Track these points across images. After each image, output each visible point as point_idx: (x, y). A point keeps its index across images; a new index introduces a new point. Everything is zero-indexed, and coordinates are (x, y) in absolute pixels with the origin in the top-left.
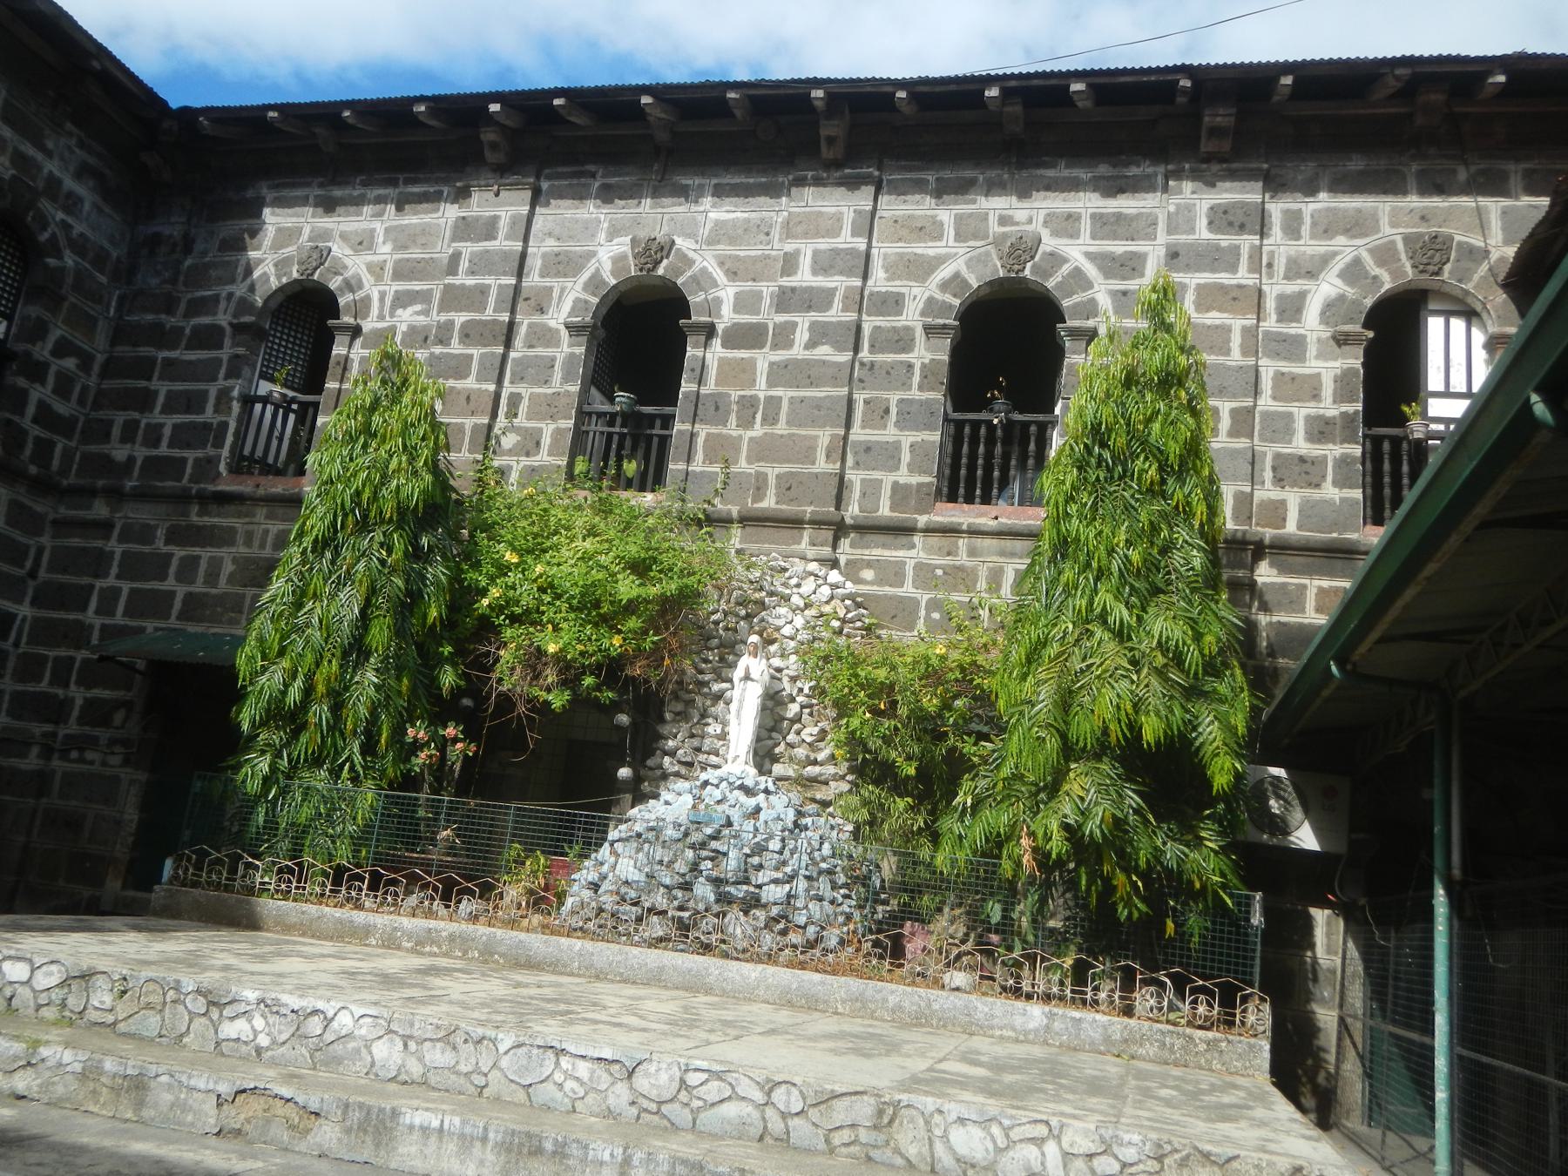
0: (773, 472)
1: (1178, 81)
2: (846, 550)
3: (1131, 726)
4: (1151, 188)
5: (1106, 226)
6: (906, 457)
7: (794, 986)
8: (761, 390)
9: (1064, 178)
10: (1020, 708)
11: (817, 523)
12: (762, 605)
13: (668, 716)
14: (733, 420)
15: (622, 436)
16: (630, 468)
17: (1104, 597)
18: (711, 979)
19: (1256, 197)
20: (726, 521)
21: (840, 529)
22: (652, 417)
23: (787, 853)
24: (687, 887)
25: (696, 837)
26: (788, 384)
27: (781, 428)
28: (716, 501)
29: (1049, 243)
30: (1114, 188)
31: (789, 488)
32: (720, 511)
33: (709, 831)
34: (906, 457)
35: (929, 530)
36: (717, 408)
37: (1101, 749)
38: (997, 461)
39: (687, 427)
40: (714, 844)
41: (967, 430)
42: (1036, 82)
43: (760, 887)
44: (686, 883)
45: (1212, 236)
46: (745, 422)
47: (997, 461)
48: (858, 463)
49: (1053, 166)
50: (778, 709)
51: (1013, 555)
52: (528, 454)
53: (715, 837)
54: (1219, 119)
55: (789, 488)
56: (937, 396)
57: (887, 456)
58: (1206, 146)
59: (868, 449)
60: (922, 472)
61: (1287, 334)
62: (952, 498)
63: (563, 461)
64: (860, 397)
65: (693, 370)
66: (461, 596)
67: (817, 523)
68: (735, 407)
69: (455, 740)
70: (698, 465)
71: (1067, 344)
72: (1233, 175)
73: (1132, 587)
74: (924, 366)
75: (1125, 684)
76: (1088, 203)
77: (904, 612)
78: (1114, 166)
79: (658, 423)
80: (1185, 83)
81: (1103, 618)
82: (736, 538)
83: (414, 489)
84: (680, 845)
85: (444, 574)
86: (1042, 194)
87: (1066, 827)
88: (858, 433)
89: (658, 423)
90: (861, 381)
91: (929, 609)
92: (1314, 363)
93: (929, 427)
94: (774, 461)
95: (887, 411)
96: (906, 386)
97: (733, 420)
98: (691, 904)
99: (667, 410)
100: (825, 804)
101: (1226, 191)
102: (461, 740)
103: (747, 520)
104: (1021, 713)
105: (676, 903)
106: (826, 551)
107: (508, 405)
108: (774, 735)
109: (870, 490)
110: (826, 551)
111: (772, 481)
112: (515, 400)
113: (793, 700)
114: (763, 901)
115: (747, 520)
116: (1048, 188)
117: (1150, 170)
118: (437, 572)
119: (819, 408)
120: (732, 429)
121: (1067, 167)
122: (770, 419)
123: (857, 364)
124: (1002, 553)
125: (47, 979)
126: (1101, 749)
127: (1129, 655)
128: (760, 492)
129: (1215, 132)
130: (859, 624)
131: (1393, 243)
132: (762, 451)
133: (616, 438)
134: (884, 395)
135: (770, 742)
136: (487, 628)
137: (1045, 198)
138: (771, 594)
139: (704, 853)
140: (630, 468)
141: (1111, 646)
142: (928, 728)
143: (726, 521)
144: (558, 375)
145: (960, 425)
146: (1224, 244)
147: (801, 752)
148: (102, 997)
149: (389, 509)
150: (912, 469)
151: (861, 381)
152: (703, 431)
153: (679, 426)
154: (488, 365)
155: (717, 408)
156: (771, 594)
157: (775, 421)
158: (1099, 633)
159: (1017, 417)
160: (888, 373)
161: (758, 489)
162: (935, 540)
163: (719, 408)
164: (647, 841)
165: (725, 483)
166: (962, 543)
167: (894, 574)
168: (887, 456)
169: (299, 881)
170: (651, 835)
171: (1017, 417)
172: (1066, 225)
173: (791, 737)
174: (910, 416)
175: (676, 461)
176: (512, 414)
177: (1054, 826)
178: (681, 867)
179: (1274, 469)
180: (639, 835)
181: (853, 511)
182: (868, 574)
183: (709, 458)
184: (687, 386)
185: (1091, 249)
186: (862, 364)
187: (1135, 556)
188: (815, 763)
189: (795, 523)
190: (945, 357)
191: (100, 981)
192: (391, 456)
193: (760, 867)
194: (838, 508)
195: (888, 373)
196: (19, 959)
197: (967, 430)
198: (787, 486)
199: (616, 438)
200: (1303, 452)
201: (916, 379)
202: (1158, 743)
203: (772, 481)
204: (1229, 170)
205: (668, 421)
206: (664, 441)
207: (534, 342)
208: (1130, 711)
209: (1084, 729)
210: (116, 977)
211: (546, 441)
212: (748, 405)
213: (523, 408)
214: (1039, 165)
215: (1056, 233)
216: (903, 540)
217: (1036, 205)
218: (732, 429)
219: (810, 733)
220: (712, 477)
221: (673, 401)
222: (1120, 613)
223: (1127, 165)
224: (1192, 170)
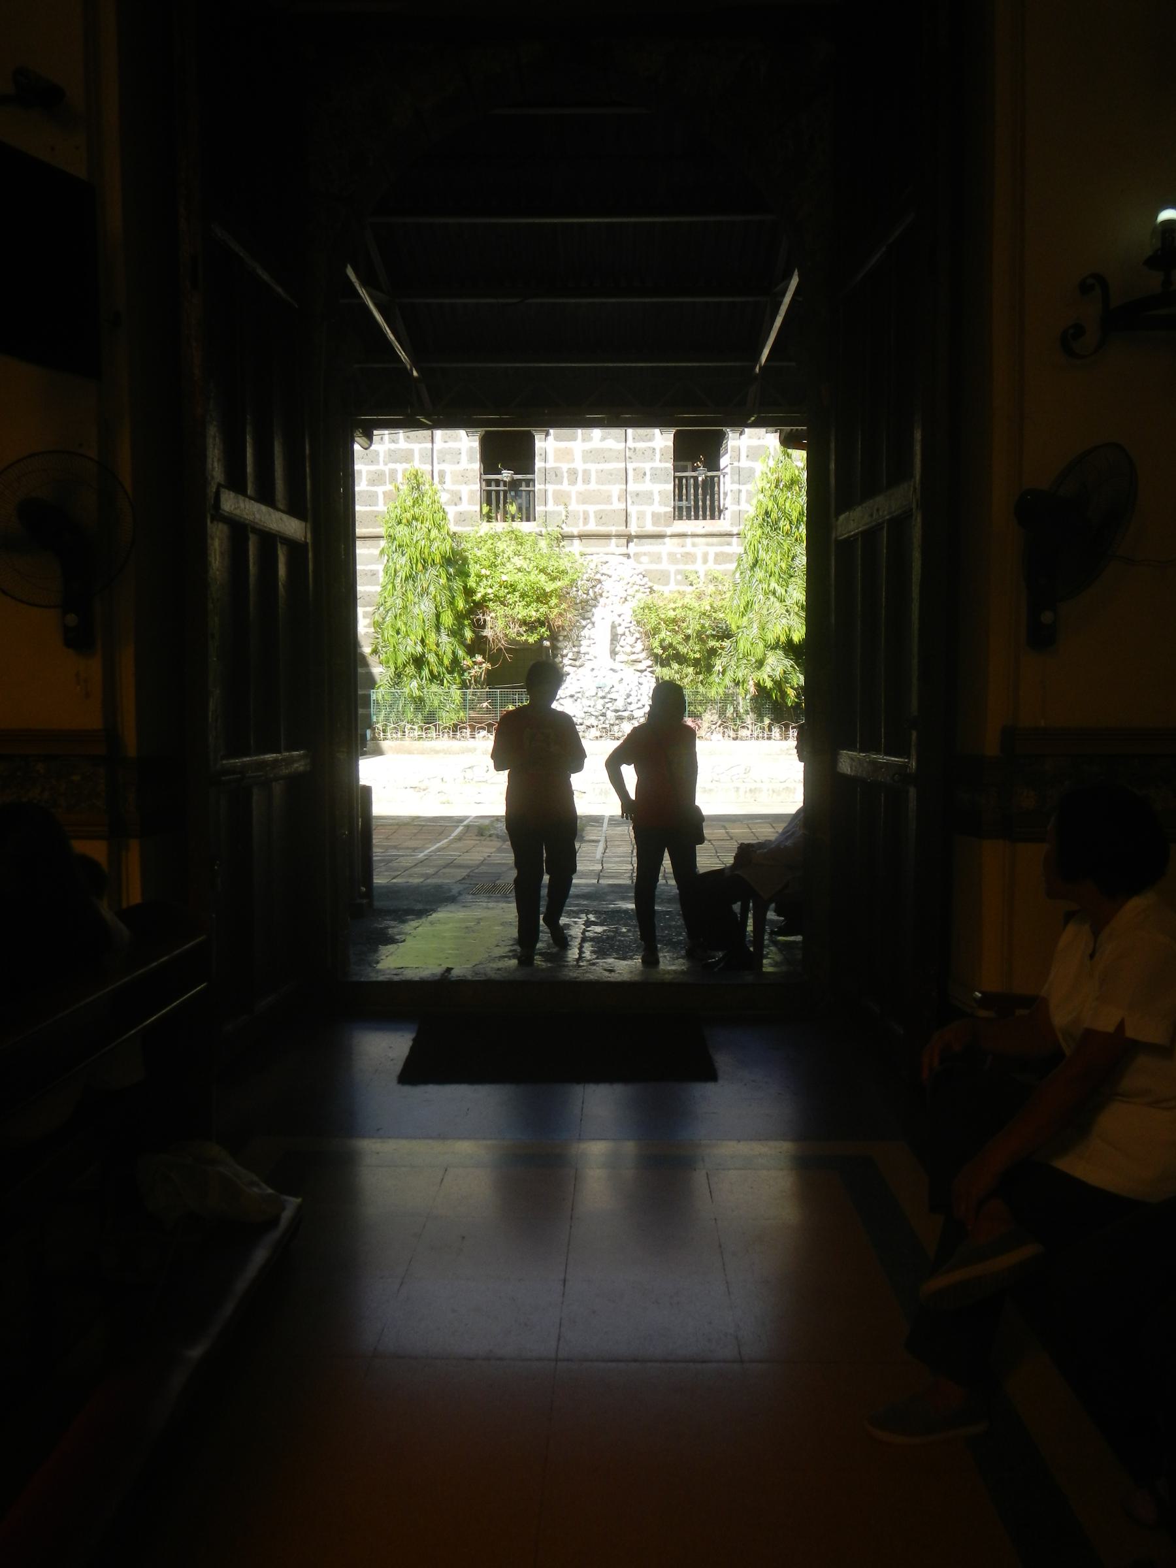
0: (592, 509)
2: (633, 548)
3: (788, 636)
6: (657, 498)
8: (579, 465)
10: (741, 630)
11: (618, 536)
12: (600, 581)
13: (561, 638)
14: (565, 481)
15: (505, 492)
16: (513, 509)
17: (773, 585)
20: (571, 537)
21: (629, 538)
22: (520, 481)
23: (639, 695)
24: (604, 715)
25: (601, 694)
26: (593, 462)
27: (593, 486)
28: (564, 526)
31: (601, 518)
32: (567, 532)
33: (607, 690)
34: (657, 498)
35: (672, 536)
36: (556, 475)
37: (775, 647)
38: (700, 497)
39: (542, 487)
40: (609, 696)
41: (684, 481)
43: (632, 711)
44: (603, 713)
46: (573, 482)
47: (700, 497)
48: (633, 502)
50: (614, 630)
51: (712, 545)
52: (456, 505)
53: (609, 693)
55: (601, 518)
56: (670, 465)
57: (647, 497)
59: (637, 495)
60: (666, 506)
62: (680, 518)
63: (478, 508)
64: (630, 466)
65: (541, 455)
66: (469, 592)
67: (618, 536)
68: (565, 475)
69: (481, 663)
70: (551, 507)
71: (730, 435)
73: (782, 578)
74: (661, 449)
75: (784, 621)
77: (663, 577)
79: (524, 484)
81: (774, 593)
82: (576, 546)
83: (447, 546)
84: (595, 697)
85: (461, 585)
87: (769, 676)
88: (632, 487)
89: (524, 484)
90: (630, 458)
91: (676, 575)
93: (666, 482)
94: (592, 503)
95: (645, 474)
96: (652, 460)
97: (565, 481)
98: (607, 722)
99: (529, 477)
100: (642, 671)
102: (484, 663)
103: (581, 537)
104: (743, 632)
105: (602, 722)
106: (624, 550)
107: (439, 476)
108: (615, 642)
109: (641, 516)
110: (624, 550)
111: (592, 515)
112: (442, 474)
113: (620, 625)
114: (635, 717)
115: (581, 537)
118: (458, 584)
119: (611, 475)
120: (565, 486)
122: (587, 481)
123: (627, 449)
124: (708, 544)
126: (775, 647)
127: (786, 608)
128: (586, 520)
130: (646, 586)
132: (585, 498)
133: (502, 493)
134: (641, 465)
135: (614, 646)
136: (480, 606)
138: (602, 574)
139: (607, 700)
140: (513, 509)
141: (777, 604)
142: (701, 637)
143: (571, 537)
144: (464, 458)
145: (680, 479)
147: (628, 649)
149: (438, 559)
150: (660, 504)
151: (630, 458)
152: (550, 488)
153: (538, 487)
154: (425, 455)
155: (556, 475)
156: (602, 574)
157: (589, 482)
158: (772, 599)
159: (710, 474)
160: (643, 453)
161: (585, 519)
162: (676, 540)
163: (557, 473)
164: (578, 698)
165: (567, 516)
166: (689, 540)
167: (657, 558)
168: (647, 497)
169: (436, 732)
170: (579, 695)
171: (710, 474)
173: (622, 643)
174: (655, 477)
175: (539, 505)
176: (442, 482)
177: (766, 677)
178: (599, 707)
180: (572, 696)
181: (633, 529)
182: (644, 559)
183: (557, 503)
184: (539, 464)
186: (630, 449)
187: (784, 565)
188: (634, 653)
189: (607, 536)
190: (671, 444)
192: (429, 531)
193: (630, 704)
194: (626, 527)
195: (643, 453)
197: (684, 481)
198: (600, 517)
199: (502, 493)
201: (658, 456)
202: (800, 641)
203: (592, 515)
205: (530, 482)
206: (531, 494)
207: (447, 440)
208: (787, 631)
209: (771, 638)
211: (465, 498)
212: (573, 473)
213: (448, 478)
216: (660, 540)
218: (565, 486)
219: (631, 640)
220: (559, 514)
221: (533, 473)
222: (780, 591)
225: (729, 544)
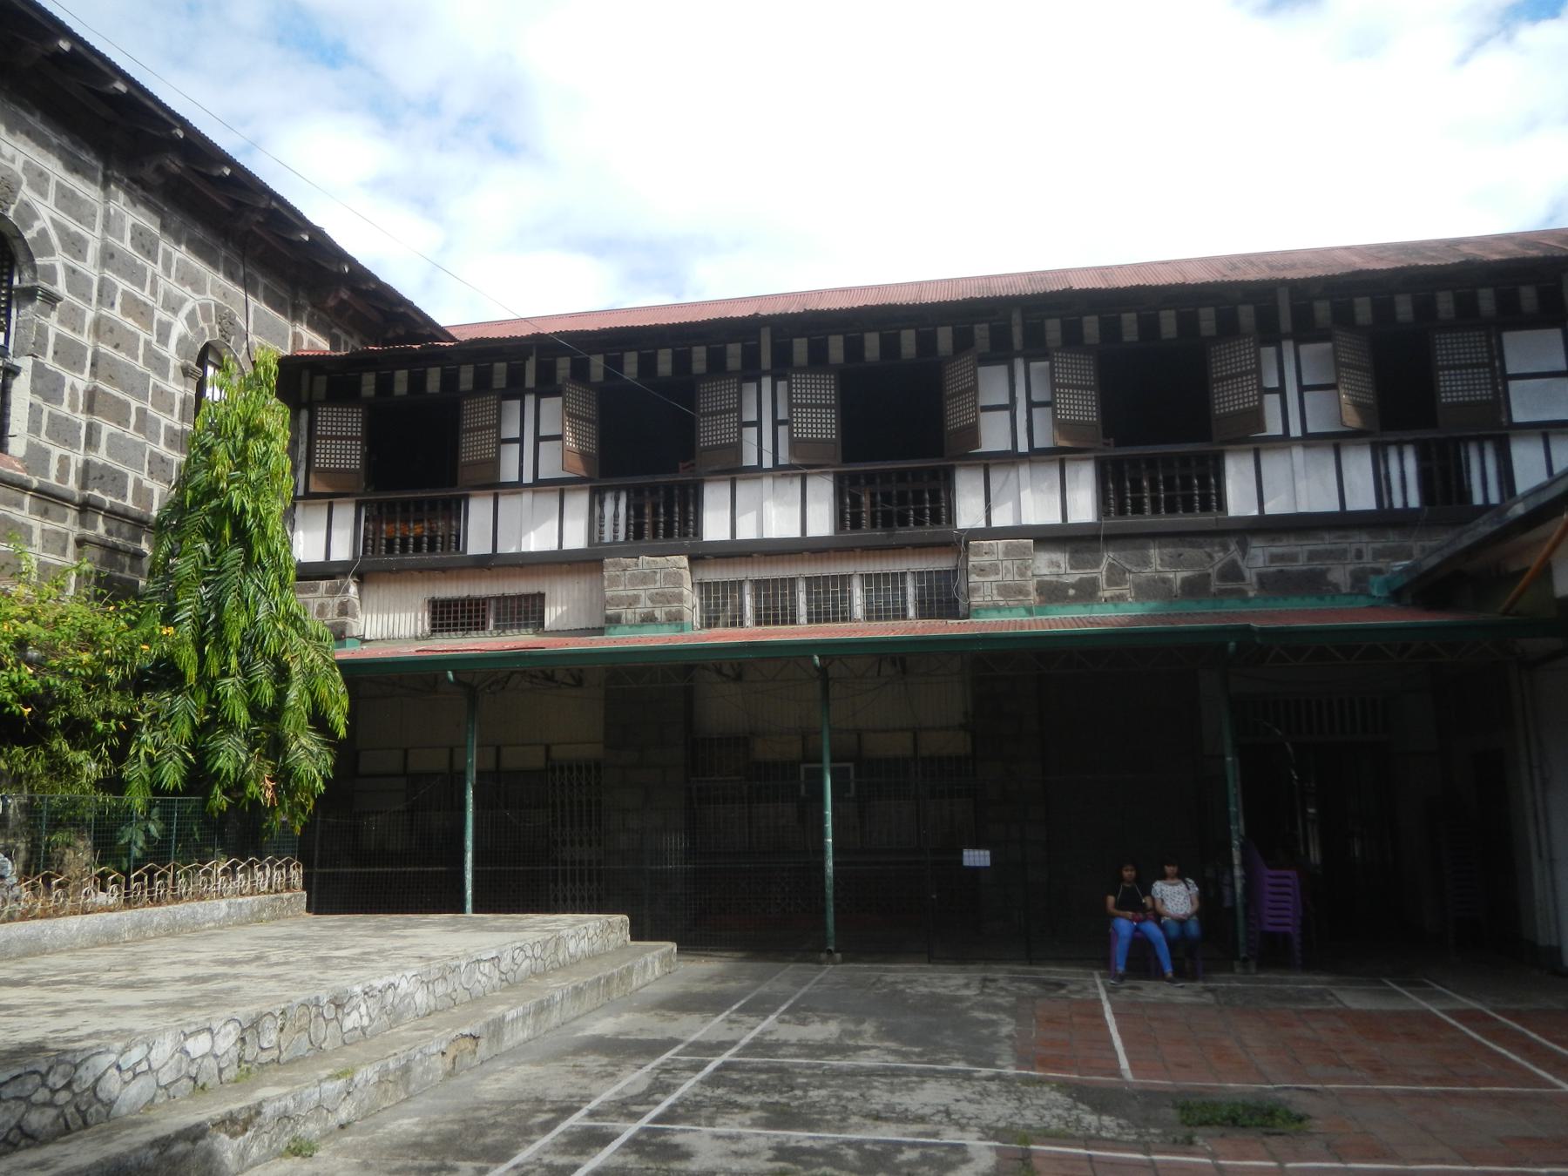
1: (175, 127)
4: (93, 180)
5: (67, 199)
7: (101, 928)
9: (40, 133)
18: (45, 940)
19: (156, 230)
29: (26, 193)
30: (74, 167)
42: (96, 61)
45: (131, 250)
49: (32, 114)
54: (173, 166)
58: (148, 173)
61: (161, 354)
71: (38, 303)
72: (147, 204)
76: (53, 167)
78: (74, 143)
80: (181, 134)
86: (24, 137)
92: (172, 384)
101: (142, 215)
116: (28, 134)
117: (94, 163)
121: (43, 121)
125: (226, 1041)
129: (160, 169)
131: (210, 305)
137: (25, 144)
146: (139, 262)
148: (270, 1037)
172: (39, 179)
179: (149, 463)
185: (55, 216)
191: (268, 1023)
196: (198, 1032)
200: (163, 453)
204: (146, 199)
210: (277, 1013)
214: (21, 105)
215: (31, 185)
217: (19, 146)
223: (81, 147)
224: (128, 186)
225: (19, 505)
